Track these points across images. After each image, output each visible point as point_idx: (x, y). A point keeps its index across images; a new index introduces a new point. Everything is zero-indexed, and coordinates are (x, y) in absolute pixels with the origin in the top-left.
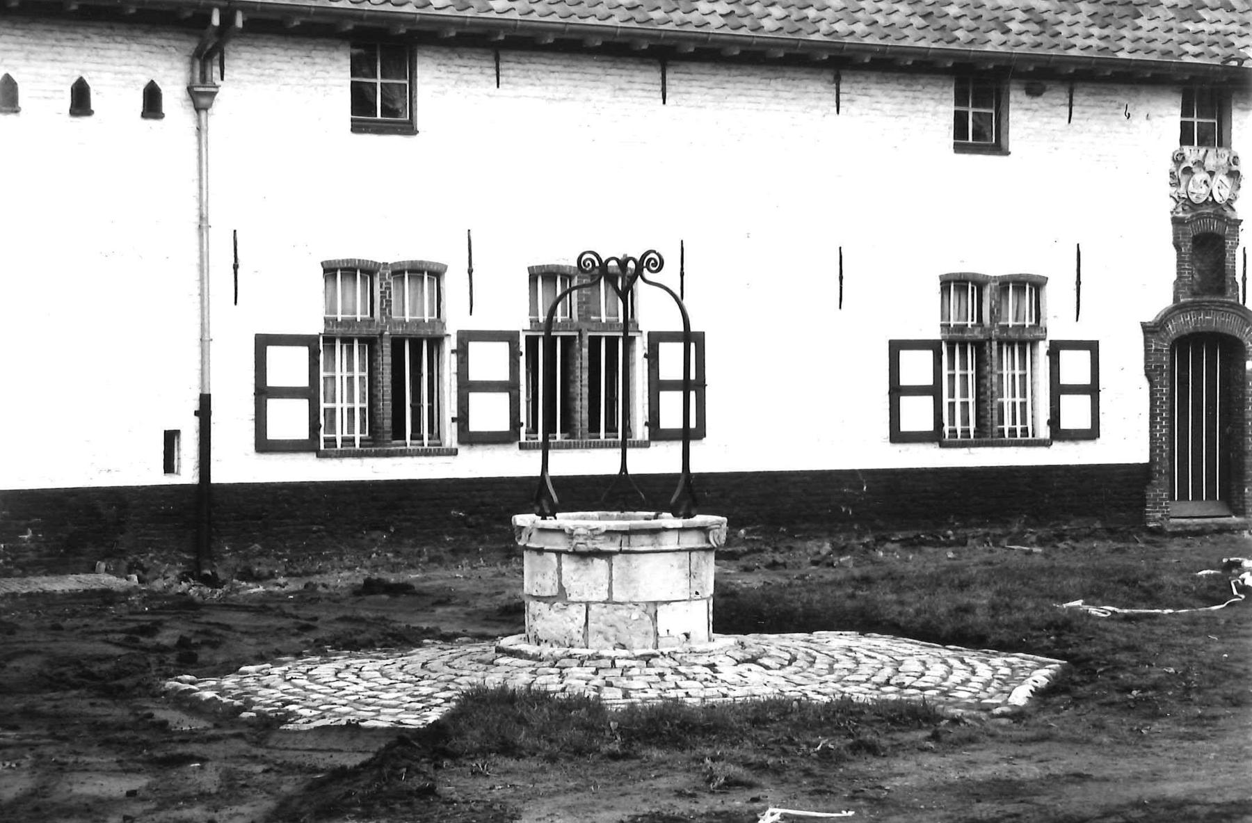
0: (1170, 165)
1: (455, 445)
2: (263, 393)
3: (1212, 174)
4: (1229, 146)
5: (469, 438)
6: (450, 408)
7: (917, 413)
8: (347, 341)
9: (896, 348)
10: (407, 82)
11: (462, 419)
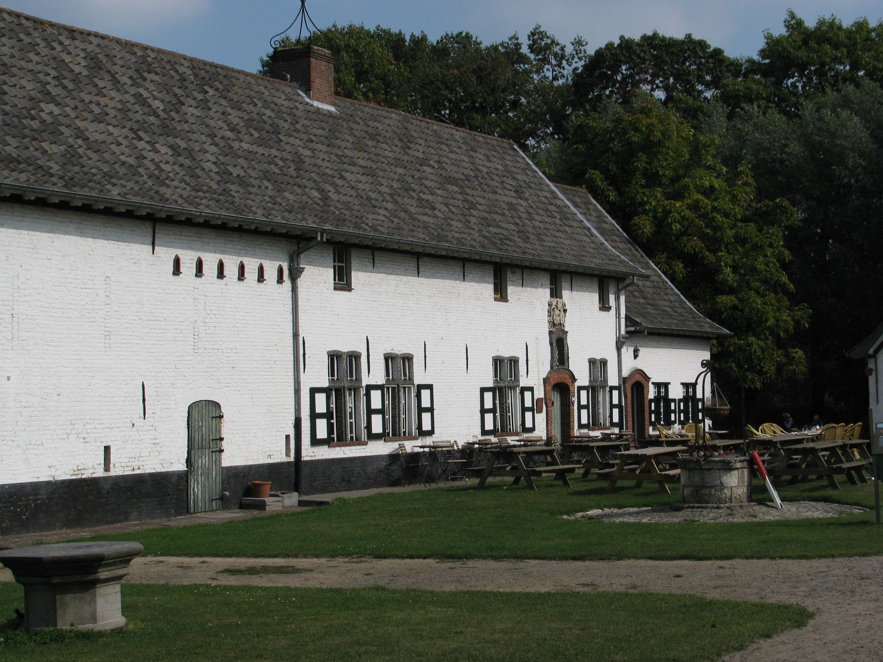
0: (547, 307)
4: (561, 297)
5: (372, 437)
6: (364, 424)
8: (350, 390)
9: (483, 390)
10: (344, 265)
11: (369, 427)
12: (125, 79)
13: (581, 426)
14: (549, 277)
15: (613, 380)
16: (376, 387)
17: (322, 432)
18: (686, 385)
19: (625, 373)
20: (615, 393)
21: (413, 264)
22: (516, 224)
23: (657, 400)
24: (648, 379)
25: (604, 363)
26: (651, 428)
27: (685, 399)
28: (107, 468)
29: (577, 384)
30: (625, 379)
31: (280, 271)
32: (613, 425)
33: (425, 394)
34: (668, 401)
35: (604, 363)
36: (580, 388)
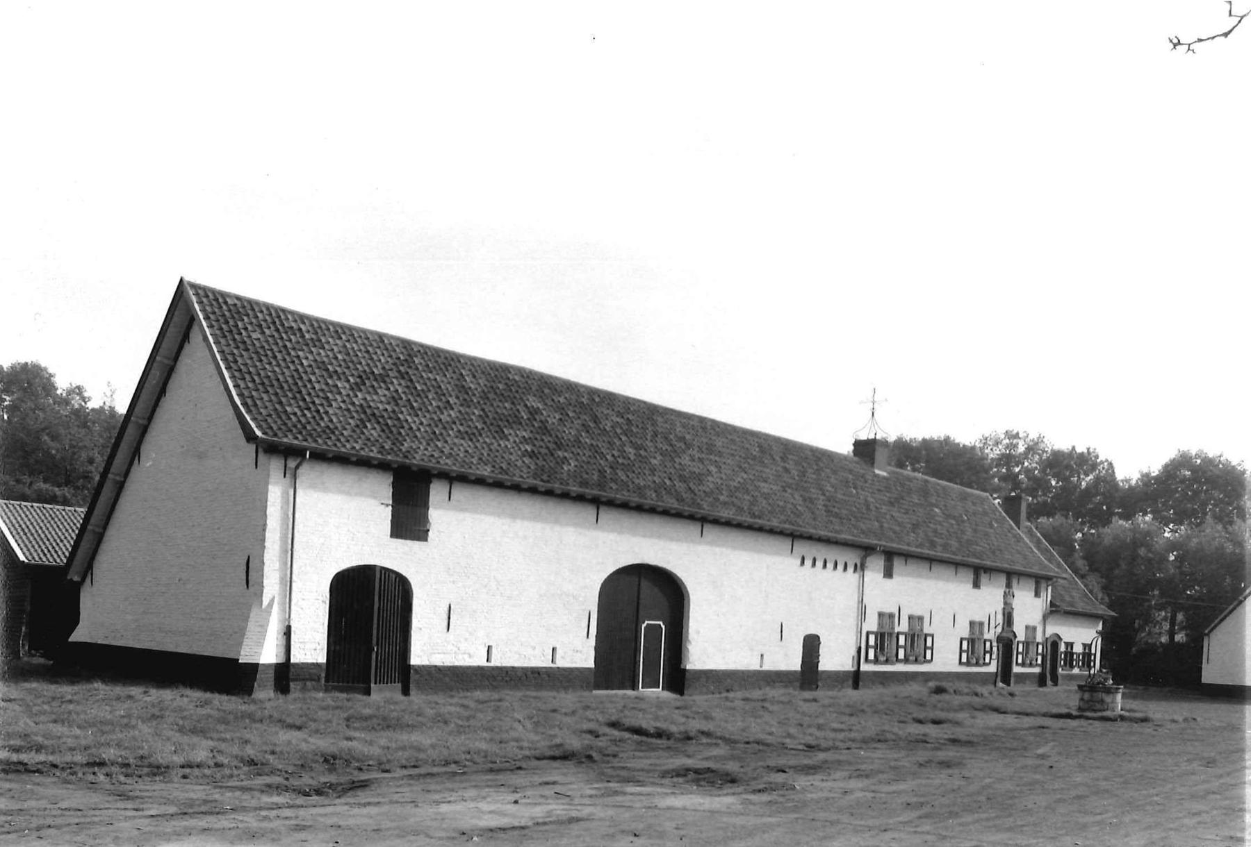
5: (898, 660)
9: (962, 640)
12: (778, 458)
15: (1039, 639)
16: (902, 633)
17: (871, 656)
18: (1085, 645)
19: (1047, 636)
20: (1040, 647)
21: (927, 566)
22: (989, 545)
23: (1066, 653)
24: (1061, 639)
25: (1034, 629)
26: (1060, 669)
27: (1084, 654)
28: (761, 667)
29: (1017, 640)
30: (1047, 639)
31: (856, 565)
32: (1037, 665)
33: (929, 640)
34: (1072, 654)
35: (1034, 629)
36: (1018, 643)
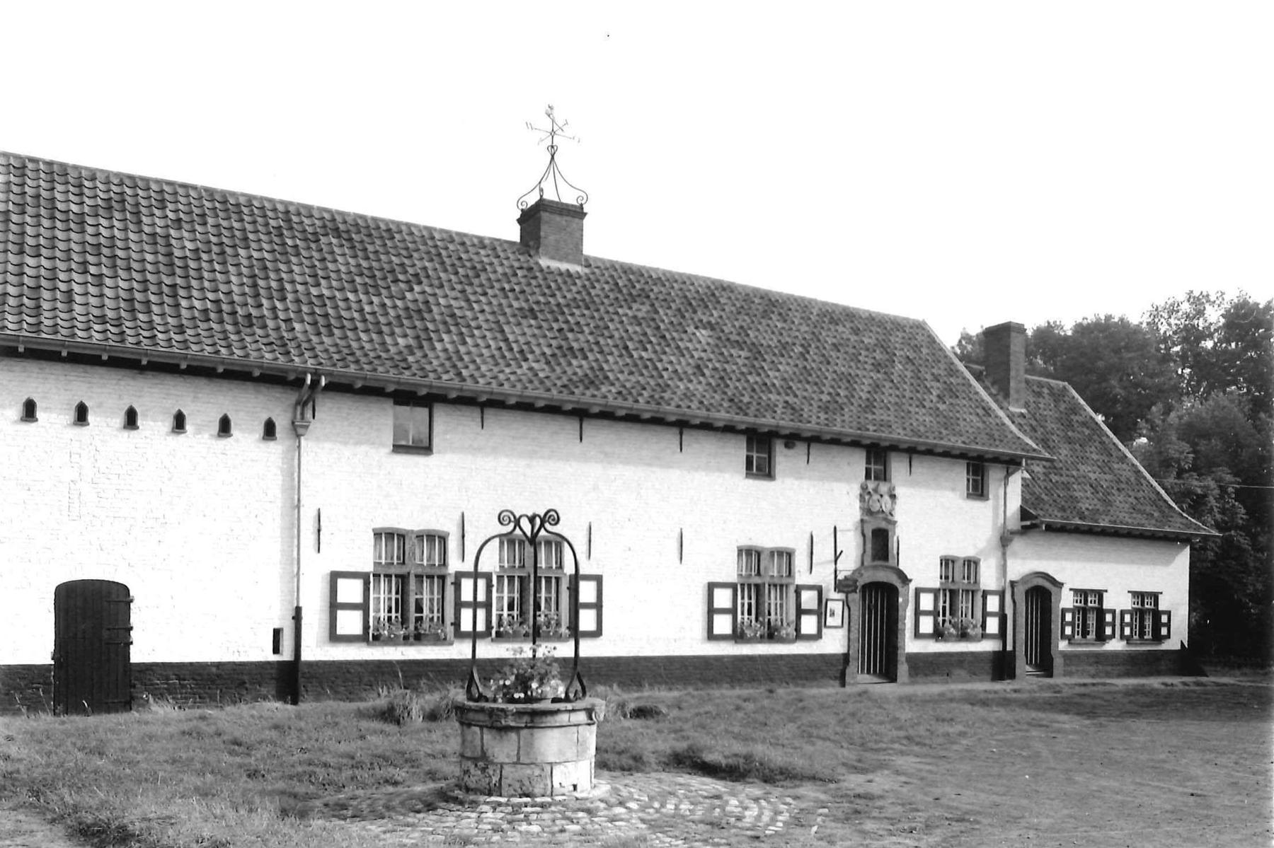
1: (452, 638)
2: (334, 606)
3: (881, 496)
4: (890, 481)
7: (723, 625)
9: (711, 587)
13: (917, 635)
14: (864, 454)
29: (912, 586)
30: (1013, 584)
34: (1101, 612)
